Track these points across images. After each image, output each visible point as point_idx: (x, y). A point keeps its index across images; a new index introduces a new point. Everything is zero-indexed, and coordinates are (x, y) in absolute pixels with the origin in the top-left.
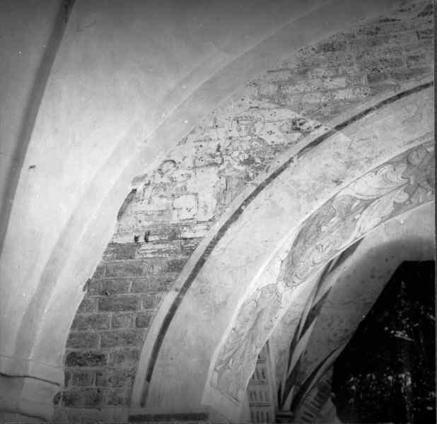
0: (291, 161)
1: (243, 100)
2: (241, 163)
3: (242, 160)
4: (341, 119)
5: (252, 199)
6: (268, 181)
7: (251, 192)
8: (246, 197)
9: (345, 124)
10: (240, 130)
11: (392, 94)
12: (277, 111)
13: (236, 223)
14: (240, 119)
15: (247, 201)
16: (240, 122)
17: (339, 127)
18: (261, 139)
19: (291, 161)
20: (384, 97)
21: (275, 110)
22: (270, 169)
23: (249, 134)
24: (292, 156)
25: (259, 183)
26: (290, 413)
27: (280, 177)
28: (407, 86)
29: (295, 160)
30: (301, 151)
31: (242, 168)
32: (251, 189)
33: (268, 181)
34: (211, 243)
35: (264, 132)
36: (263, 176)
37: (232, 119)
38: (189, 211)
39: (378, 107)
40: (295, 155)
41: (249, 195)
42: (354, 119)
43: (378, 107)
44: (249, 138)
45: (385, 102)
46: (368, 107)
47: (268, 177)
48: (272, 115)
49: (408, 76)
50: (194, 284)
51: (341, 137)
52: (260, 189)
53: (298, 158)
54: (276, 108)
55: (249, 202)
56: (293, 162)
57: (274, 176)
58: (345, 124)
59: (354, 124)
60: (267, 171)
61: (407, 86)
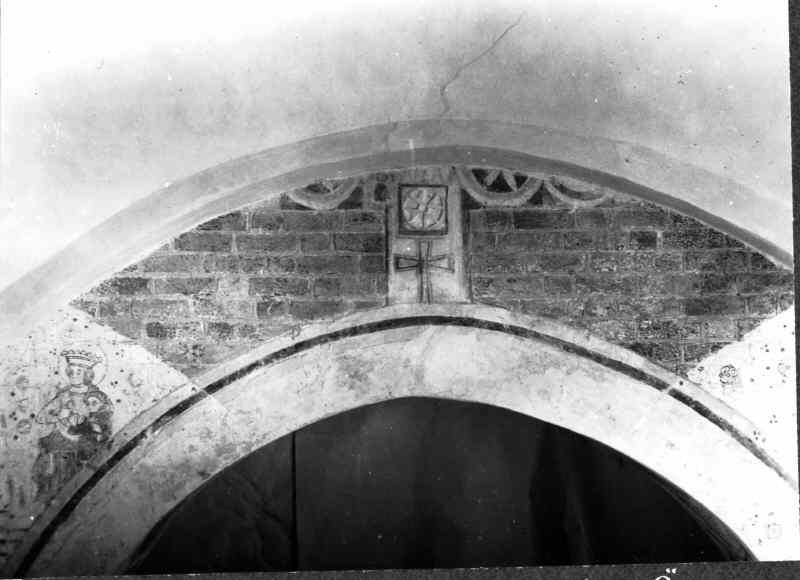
0: (143, 434)
2: (73, 430)
4: (213, 375)
10: (70, 374)
11: (287, 342)
12: (126, 347)
16: (72, 361)
17: (212, 388)
18: (102, 394)
19: (143, 434)
23: (87, 382)
25: (99, 465)
28: (310, 331)
30: (158, 421)
31: (74, 438)
39: (268, 360)
42: (233, 377)
43: (268, 360)
44: (84, 389)
45: (277, 355)
46: (252, 360)
47: (110, 456)
49: (310, 314)
57: (120, 456)
60: (109, 447)
61: (310, 331)
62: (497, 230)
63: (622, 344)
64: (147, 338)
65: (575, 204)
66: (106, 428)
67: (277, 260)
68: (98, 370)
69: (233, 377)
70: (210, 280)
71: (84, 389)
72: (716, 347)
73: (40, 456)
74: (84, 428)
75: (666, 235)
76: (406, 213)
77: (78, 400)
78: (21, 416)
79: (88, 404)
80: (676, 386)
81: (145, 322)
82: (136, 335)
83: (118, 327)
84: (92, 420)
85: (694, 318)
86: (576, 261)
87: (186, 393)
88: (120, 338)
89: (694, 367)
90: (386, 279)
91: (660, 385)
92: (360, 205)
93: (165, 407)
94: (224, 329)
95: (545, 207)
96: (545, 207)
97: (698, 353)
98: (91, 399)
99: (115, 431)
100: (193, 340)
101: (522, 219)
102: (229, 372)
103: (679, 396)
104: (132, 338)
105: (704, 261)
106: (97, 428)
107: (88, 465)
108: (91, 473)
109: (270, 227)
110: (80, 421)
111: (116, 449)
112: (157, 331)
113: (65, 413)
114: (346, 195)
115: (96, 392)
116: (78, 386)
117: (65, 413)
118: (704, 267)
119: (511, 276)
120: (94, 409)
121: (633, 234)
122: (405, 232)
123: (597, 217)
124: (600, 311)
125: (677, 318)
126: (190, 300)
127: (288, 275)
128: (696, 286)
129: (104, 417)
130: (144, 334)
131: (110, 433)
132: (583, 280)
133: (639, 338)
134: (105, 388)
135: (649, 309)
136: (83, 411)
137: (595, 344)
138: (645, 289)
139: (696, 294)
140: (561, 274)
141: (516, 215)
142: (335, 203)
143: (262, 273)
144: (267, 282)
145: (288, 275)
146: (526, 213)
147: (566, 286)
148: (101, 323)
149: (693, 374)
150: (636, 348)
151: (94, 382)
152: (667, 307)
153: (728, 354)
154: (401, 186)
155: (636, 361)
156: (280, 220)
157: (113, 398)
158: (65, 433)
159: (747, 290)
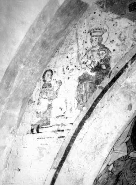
0: (126, 66)
1: (95, 13)
2: (93, 70)
3: (93, 67)
5: (100, 100)
6: (110, 84)
7: (99, 94)
8: (95, 99)
10: (92, 41)
13: (89, 119)
14: (92, 31)
15: (96, 101)
16: (92, 34)
18: (106, 48)
19: (126, 66)
21: (116, 20)
22: (112, 73)
24: (127, 61)
27: (120, 80)
29: (129, 65)
32: (98, 92)
33: (110, 84)
34: (74, 134)
35: (108, 42)
36: (107, 81)
37: (87, 32)
38: (61, 110)
40: (129, 61)
41: (97, 97)
44: (98, 47)
47: (110, 81)
48: (114, 25)
50: (65, 164)
52: (104, 91)
53: (132, 63)
54: (117, 18)
55: (98, 103)
56: (128, 67)
57: (114, 80)
60: (110, 76)
64: (129, 12)
66: (108, 66)
71: (98, 47)
73: (79, 85)
74: (98, 68)
77: (95, 54)
78: (70, 67)
79: (100, 55)
82: (123, 13)
83: (114, 11)
84: (102, 63)
88: (115, 16)
98: (101, 52)
99: (112, 65)
106: (104, 67)
107: (100, 87)
108: (101, 91)
110: (96, 65)
111: (112, 76)
115: (104, 48)
116: (95, 47)
117: (89, 62)
129: (107, 61)
130: (127, 11)
131: (110, 69)
151: (102, 43)
157: (111, 49)
158: (89, 71)
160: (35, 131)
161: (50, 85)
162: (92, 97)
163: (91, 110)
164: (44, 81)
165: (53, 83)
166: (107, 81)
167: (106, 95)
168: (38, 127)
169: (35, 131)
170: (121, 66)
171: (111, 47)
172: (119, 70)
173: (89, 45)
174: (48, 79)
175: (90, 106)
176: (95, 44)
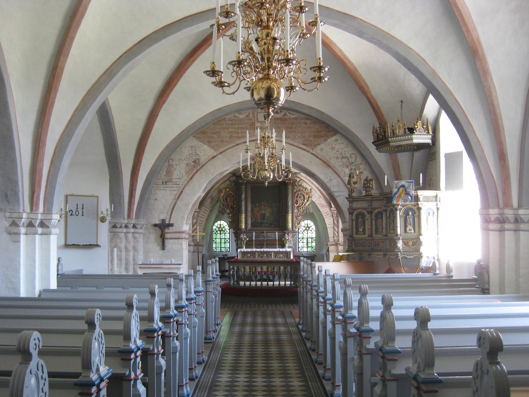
4: (220, 151)
6: (200, 168)
9: (222, 152)
10: (192, 150)
17: (220, 153)
20: (233, 145)
26: (198, 210)
31: (193, 163)
32: (195, 171)
33: (200, 168)
36: (199, 167)
42: (224, 151)
45: (233, 147)
50: (180, 197)
51: (220, 156)
52: (198, 171)
57: (202, 167)
58: (222, 152)
59: (225, 152)
61: (239, 142)
62: (277, 122)
63: (301, 144)
65: (292, 116)
66: (199, 161)
67: (233, 127)
68: (197, 150)
69: (224, 151)
70: (219, 132)
72: (319, 144)
74: (195, 162)
75: (309, 122)
76: (258, 118)
77: (194, 156)
80: (312, 152)
81: (207, 140)
85: (315, 139)
86: (292, 127)
87: (215, 154)
89: (315, 148)
90: (254, 131)
91: (309, 152)
92: (249, 116)
93: (211, 157)
94: (223, 141)
95: (286, 117)
96: (286, 117)
97: (316, 146)
99: (201, 162)
100: (216, 144)
101: (281, 119)
102: (224, 150)
103: (312, 154)
104: (205, 144)
105: (316, 127)
106: (197, 161)
109: (232, 121)
112: (209, 142)
113: (191, 158)
114: (246, 114)
117: (191, 158)
118: (317, 129)
119: (279, 130)
120: (197, 158)
121: (303, 122)
122: (258, 122)
123: (296, 119)
124: (297, 137)
125: (311, 139)
126: (216, 135)
127: (235, 130)
128: (315, 132)
129: (199, 160)
130: (207, 143)
132: (294, 131)
133: (305, 143)
134: (199, 153)
135: (306, 137)
136: (194, 158)
137: (296, 144)
138: (306, 133)
139: (315, 134)
140: (289, 130)
141: (280, 118)
142: (244, 116)
143: (230, 130)
144: (231, 132)
145: (235, 130)
146: (282, 118)
147: (290, 132)
148: (198, 141)
149: (315, 149)
150: (304, 144)
152: (310, 136)
153: (322, 146)
154: (257, 113)
155: (304, 147)
156: (234, 120)
157: (200, 155)
158: (191, 163)
159: (325, 133)
160: (164, 184)
161: (172, 165)
162: (192, 173)
163: (191, 178)
164: (169, 163)
165: (173, 164)
166: (199, 167)
167: (198, 172)
168: (166, 182)
169: (164, 184)
170: (205, 162)
171: (200, 155)
172: (204, 164)
173: (191, 152)
174: (171, 163)
175: (192, 175)
176: (193, 152)
